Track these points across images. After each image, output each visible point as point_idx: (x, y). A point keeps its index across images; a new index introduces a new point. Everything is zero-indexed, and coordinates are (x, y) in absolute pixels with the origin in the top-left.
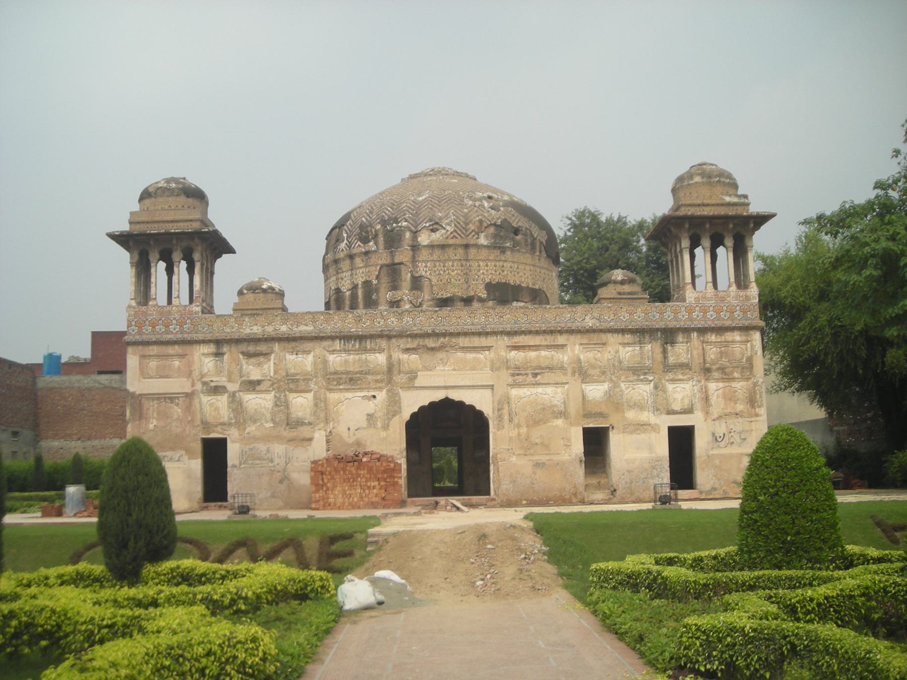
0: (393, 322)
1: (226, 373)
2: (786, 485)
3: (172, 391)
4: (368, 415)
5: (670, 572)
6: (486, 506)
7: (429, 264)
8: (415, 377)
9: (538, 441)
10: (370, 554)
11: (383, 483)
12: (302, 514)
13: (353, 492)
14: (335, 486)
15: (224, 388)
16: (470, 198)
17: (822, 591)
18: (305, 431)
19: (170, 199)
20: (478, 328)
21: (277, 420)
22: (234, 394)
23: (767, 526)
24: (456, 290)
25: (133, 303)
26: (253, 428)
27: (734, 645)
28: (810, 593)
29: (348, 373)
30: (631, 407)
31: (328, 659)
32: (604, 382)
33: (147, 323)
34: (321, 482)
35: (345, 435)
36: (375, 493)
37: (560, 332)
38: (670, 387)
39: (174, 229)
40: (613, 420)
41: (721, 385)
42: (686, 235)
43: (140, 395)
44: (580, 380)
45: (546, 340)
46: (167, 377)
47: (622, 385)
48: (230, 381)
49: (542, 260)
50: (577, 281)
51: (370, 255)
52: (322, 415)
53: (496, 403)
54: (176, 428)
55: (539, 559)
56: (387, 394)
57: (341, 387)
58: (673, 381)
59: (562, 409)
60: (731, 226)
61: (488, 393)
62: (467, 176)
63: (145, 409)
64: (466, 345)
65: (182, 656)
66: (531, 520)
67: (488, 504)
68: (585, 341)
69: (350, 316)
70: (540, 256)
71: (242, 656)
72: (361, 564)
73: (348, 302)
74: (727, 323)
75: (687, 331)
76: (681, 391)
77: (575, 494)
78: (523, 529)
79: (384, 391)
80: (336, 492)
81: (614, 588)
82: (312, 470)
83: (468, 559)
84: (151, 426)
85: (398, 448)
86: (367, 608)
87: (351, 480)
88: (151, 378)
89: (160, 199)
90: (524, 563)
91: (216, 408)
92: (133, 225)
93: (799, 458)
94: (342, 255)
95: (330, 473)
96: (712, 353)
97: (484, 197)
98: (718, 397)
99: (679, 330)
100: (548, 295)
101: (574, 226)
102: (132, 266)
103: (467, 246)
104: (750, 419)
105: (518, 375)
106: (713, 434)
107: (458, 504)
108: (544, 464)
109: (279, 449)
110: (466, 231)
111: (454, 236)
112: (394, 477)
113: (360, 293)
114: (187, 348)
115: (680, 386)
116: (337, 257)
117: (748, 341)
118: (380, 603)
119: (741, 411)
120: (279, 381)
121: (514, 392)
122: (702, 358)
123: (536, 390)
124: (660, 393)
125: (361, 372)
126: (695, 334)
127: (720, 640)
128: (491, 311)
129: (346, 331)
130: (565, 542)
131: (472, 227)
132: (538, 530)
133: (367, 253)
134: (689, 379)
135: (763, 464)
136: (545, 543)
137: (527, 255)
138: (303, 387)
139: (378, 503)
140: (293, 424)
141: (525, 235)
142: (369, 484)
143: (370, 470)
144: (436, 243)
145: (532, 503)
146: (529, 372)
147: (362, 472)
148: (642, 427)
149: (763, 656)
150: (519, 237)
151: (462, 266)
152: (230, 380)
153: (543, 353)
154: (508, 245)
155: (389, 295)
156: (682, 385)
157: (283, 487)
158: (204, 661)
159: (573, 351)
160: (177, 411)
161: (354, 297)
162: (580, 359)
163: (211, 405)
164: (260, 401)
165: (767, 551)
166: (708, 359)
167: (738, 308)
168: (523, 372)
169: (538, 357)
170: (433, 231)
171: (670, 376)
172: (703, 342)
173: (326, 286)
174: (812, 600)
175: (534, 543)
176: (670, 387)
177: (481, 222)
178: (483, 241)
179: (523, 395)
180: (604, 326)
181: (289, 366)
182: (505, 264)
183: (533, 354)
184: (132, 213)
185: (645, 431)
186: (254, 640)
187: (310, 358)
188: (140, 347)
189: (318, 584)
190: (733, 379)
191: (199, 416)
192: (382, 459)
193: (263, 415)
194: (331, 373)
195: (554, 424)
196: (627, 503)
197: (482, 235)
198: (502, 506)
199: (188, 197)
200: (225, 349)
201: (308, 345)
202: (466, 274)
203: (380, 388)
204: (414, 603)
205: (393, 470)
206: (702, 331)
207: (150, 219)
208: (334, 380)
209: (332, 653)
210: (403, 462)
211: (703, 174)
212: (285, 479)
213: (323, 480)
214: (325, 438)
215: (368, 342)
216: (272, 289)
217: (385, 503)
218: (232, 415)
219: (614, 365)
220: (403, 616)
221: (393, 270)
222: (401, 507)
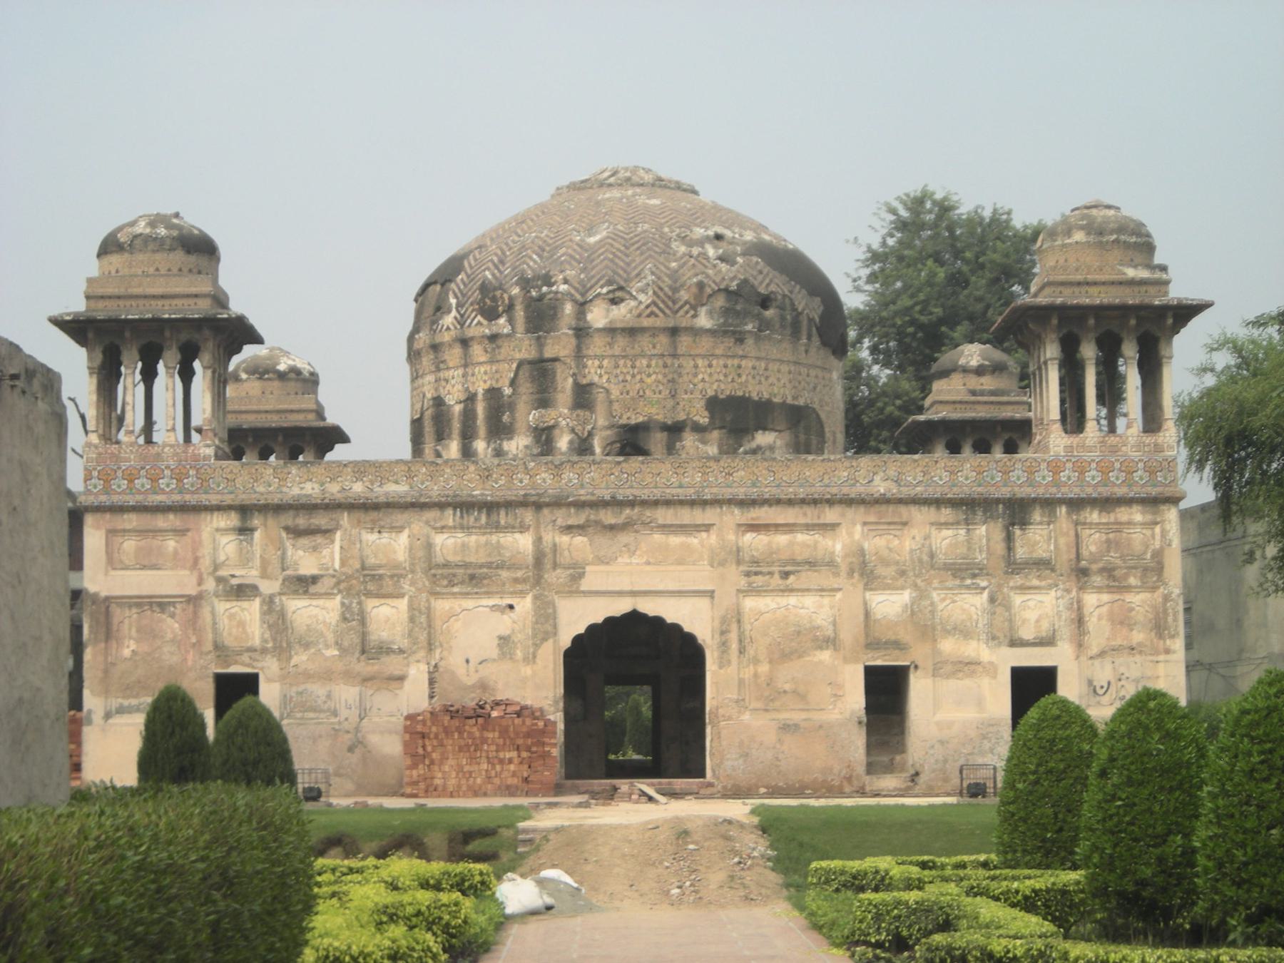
0: (545, 480)
1: (257, 562)
2: (1050, 772)
3: (164, 593)
4: (500, 638)
5: (896, 871)
6: (697, 795)
7: (605, 362)
8: (581, 575)
9: (787, 687)
10: (522, 856)
11: (525, 754)
12: (408, 803)
13: (475, 768)
14: (444, 758)
15: (254, 588)
16: (683, 239)
17: (1039, 884)
18: (391, 664)
19: (158, 256)
20: (690, 493)
21: (346, 644)
22: (271, 597)
23: (1025, 820)
24: (654, 411)
25: (94, 438)
26: (304, 658)
27: (900, 917)
28: (1016, 885)
29: (466, 565)
30: (949, 632)
31: (509, 942)
32: (903, 588)
33: (119, 473)
34: (420, 751)
35: (461, 671)
36: (512, 771)
37: (831, 502)
38: (1017, 599)
39: (168, 311)
40: (916, 654)
41: (1106, 597)
42: (1054, 336)
43: (107, 598)
44: (861, 586)
45: (805, 514)
46: (154, 567)
47: (935, 595)
48: (264, 575)
49: (813, 351)
50: (904, 348)
51: (499, 342)
52: (423, 637)
53: (717, 623)
54: (170, 656)
55: (758, 865)
56: (534, 603)
57: (456, 589)
58: (1023, 589)
59: (830, 633)
60: (1133, 322)
61: (704, 603)
62: (679, 187)
63: (115, 621)
64: (668, 522)
65: (395, 914)
66: (759, 815)
67: (702, 792)
68: (872, 519)
69: (472, 468)
70: (808, 346)
71: (447, 917)
72: (512, 869)
73: (456, 425)
74: (1121, 491)
75: (1049, 504)
76: (1039, 607)
77: (849, 779)
78: (742, 826)
79: (529, 598)
80: (447, 768)
81: (837, 890)
82: (406, 729)
83: (661, 863)
84: (127, 652)
85: (551, 695)
86: (534, 913)
87: (472, 749)
88: (126, 568)
89: (141, 257)
90: (737, 868)
91: (244, 622)
92: (93, 304)
93: (1067, 738)
94: (447, 337)
95: (436, 737)
96: (1093, 542)
97: (708, 239)
98: (1100, 618)
99: (1035, 500)
100: (823, 416)
101: (902, 225)
102: (91, 374)
103: (674, 332)
104: (1155, 658)
105: (756, 574)
106: (1090, 682)
107: (651, 792)
108: (796, 725)
109: (347, 694)
110: (674, 302)
111: (652, 313)
112: (544, 744)
113: (480, 409)
114: (191, 519)
115: (1034, 599)
116: (438, 339)
117: (1157, 523)
118: (549, 908)
119: (1140, 644)
120: (349, 577)
121: (750, 603)
122: (1074, 550)
123: (794, 597)
124: (999, 610)
125: (489, 565)
126: (1064, 509)
127: (888, 912)
128: (712, 464)
129: (464, 494)
130: (801, 845)
131: (684, 295)
132: (764, 829)
133: (493, 338)
134: (1050, 587)
135: (1025, 744)
136: (772, 847)
137: (786, 345)
138: (390, 590)
139: (517, 788)
140: (369, 649)
141: (782, 308)
142: (501, 755)
143: (504, 732)
144: (619, 325)
145: (774, 792)
146: (776, 569)
147: (490, 735)
148: (968, 666)
149: (923, 925)
150: (769, 313)
151: (665, 366)
152: (264, 575)
153: (801, 537)
154: (749, 327)
155: (533, 416)
156: (1039, 597)
157: (354, 758)
158: (414, 919)
159: (850, 534)
160: (171, 626)
161: (468, 415)
162: (862, 552)
163: (232, 617)
164: (316, 611)
165: (1024, 851)
166: (1085, 553)
167: (1141, 465)
168: (765, 570)
169: (791, 544)
170: (614, 302)
171: (1018, 580)
172: (1077, 524)
173: (413, 389)
174: (1017, 892)
175: (759, 846)
176: (1017, 599)
177: (701, 286)
178: (704, 321)
179: (763, 609)
180: (906, 492)
181: (368, 552)
182: (744, 363)
183: (782, 539)
184: (90, 281)
185: (972, 674)
186: (456, 904)
187: (404, 538)
188: (108, 516)
189: (478, 878)
190: (1128, 589)
191: (210, 636)
192: (526, 713)
193: (322, 634)
194: (438, 566)
195: (816, 659)
196: (937, 795)
197: (703, 311)
198: (725, 796)
199: (189, 252)
200: (256, 521)
201: (399, 518)
202: (673, 381)
203: (521, 592)
204: (591, 908)
205: (543, 732)
206: (1076, 504)
207: (122, 291)
208: (444, 577)
209: (511, 939)
210: (558, 718)
211: (1090, 228)
212: (357, 744)
213: (424, 747)
214: (426, 676)
215: (502, 513)
216: (296, 371)
217: (527, 786)
218: (267, 635)
219: (920, 561)
220: (579, 920)
221: (540, 372)
222: (555, 796)
